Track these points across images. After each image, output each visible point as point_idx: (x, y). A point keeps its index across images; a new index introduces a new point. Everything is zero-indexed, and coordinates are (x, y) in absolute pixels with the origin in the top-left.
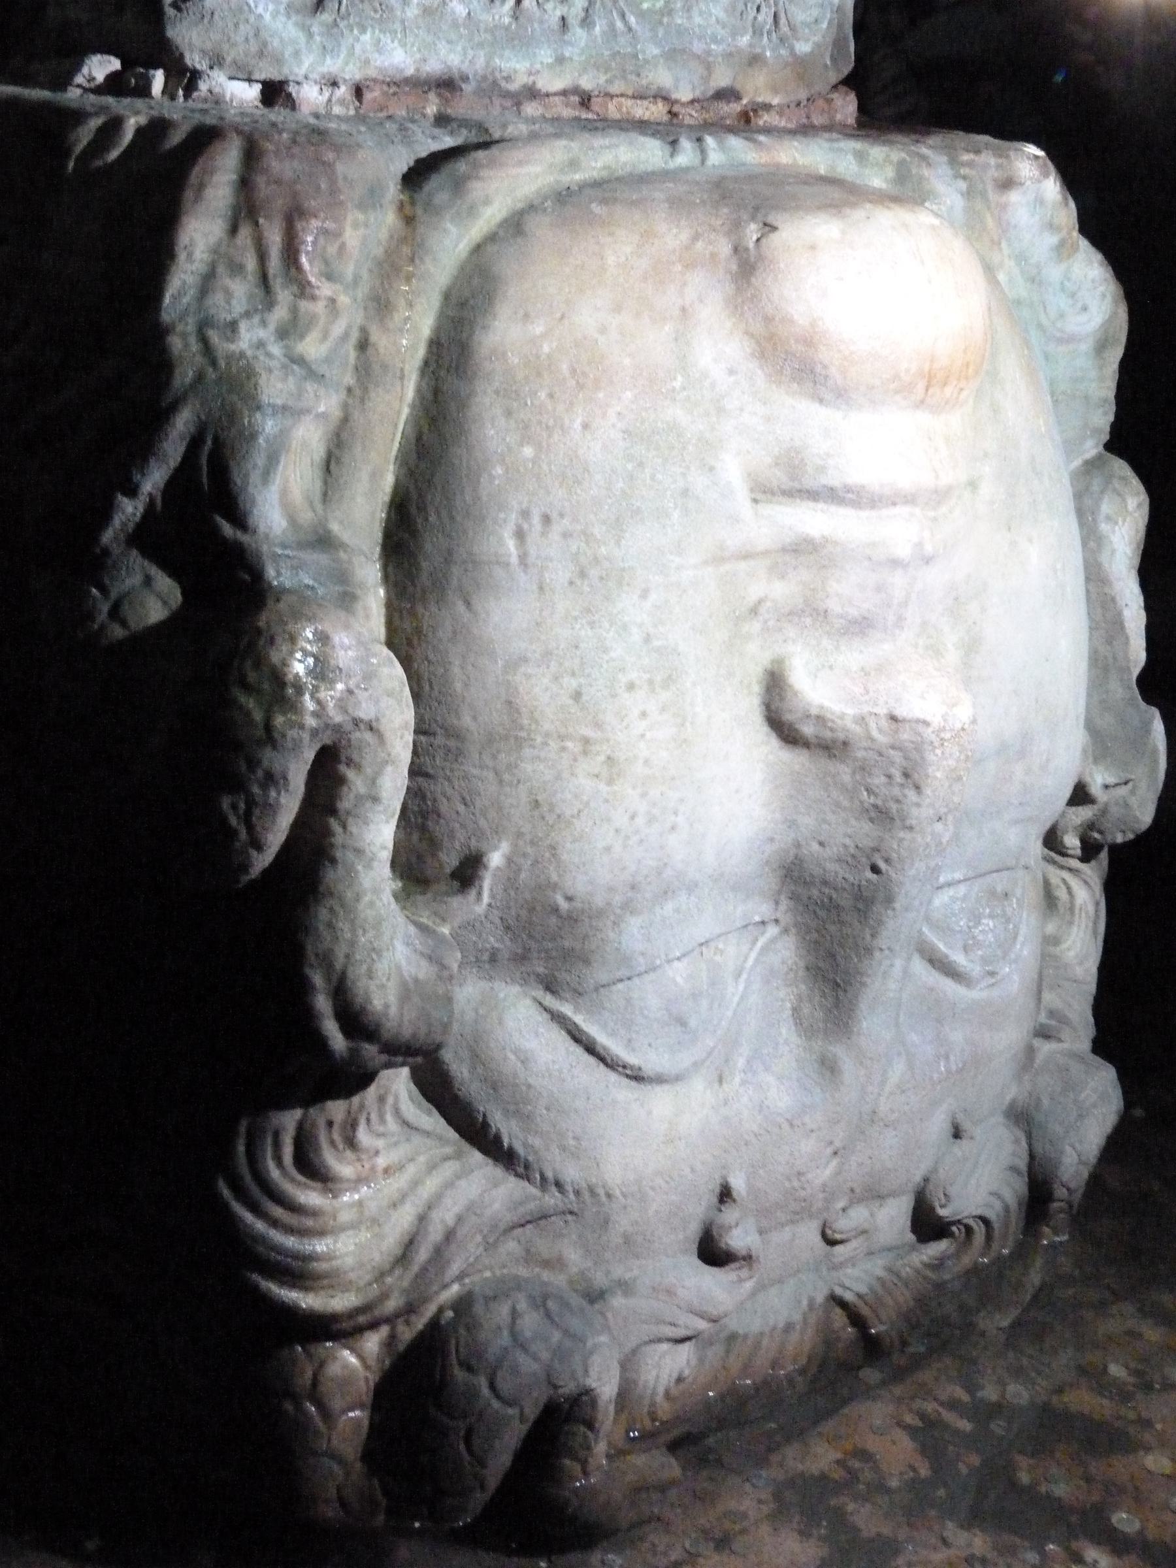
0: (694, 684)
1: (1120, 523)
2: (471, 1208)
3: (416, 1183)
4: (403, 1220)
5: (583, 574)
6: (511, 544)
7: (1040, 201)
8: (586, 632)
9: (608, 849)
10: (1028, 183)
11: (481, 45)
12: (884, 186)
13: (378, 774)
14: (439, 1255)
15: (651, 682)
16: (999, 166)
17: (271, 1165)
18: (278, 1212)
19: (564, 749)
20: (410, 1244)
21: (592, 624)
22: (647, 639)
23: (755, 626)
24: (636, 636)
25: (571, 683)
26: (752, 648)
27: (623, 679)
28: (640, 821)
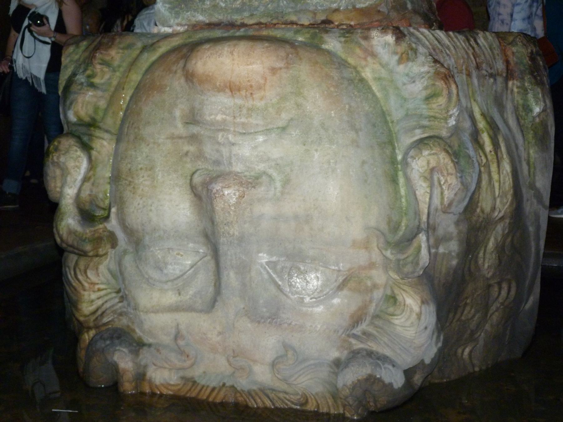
0: (159, 171)
1: (417, 159)
2: (113, 306)
3: (106, 295)
4: (100, 302)
5: (136, 138)
6: (126, 129)
7: (387, 44)
8: (134, 153)
9: (133, 212)
10: (376, 38)
11: (229, 14)
12: (304, 40)
13: (67, 176)
14: (102, 314)
15: (146, 168)
16: (361, 33)
17: (69, 276)
18: (73, 289)
19: (125, 183)
20: (97, 310)
21: (135, 151)
22: (147, 157)
23: (188, 160)
24: (144, 155)
25: (129, 166)
26: (189, 166)
27: (140, 166)
28: (141, 206)
